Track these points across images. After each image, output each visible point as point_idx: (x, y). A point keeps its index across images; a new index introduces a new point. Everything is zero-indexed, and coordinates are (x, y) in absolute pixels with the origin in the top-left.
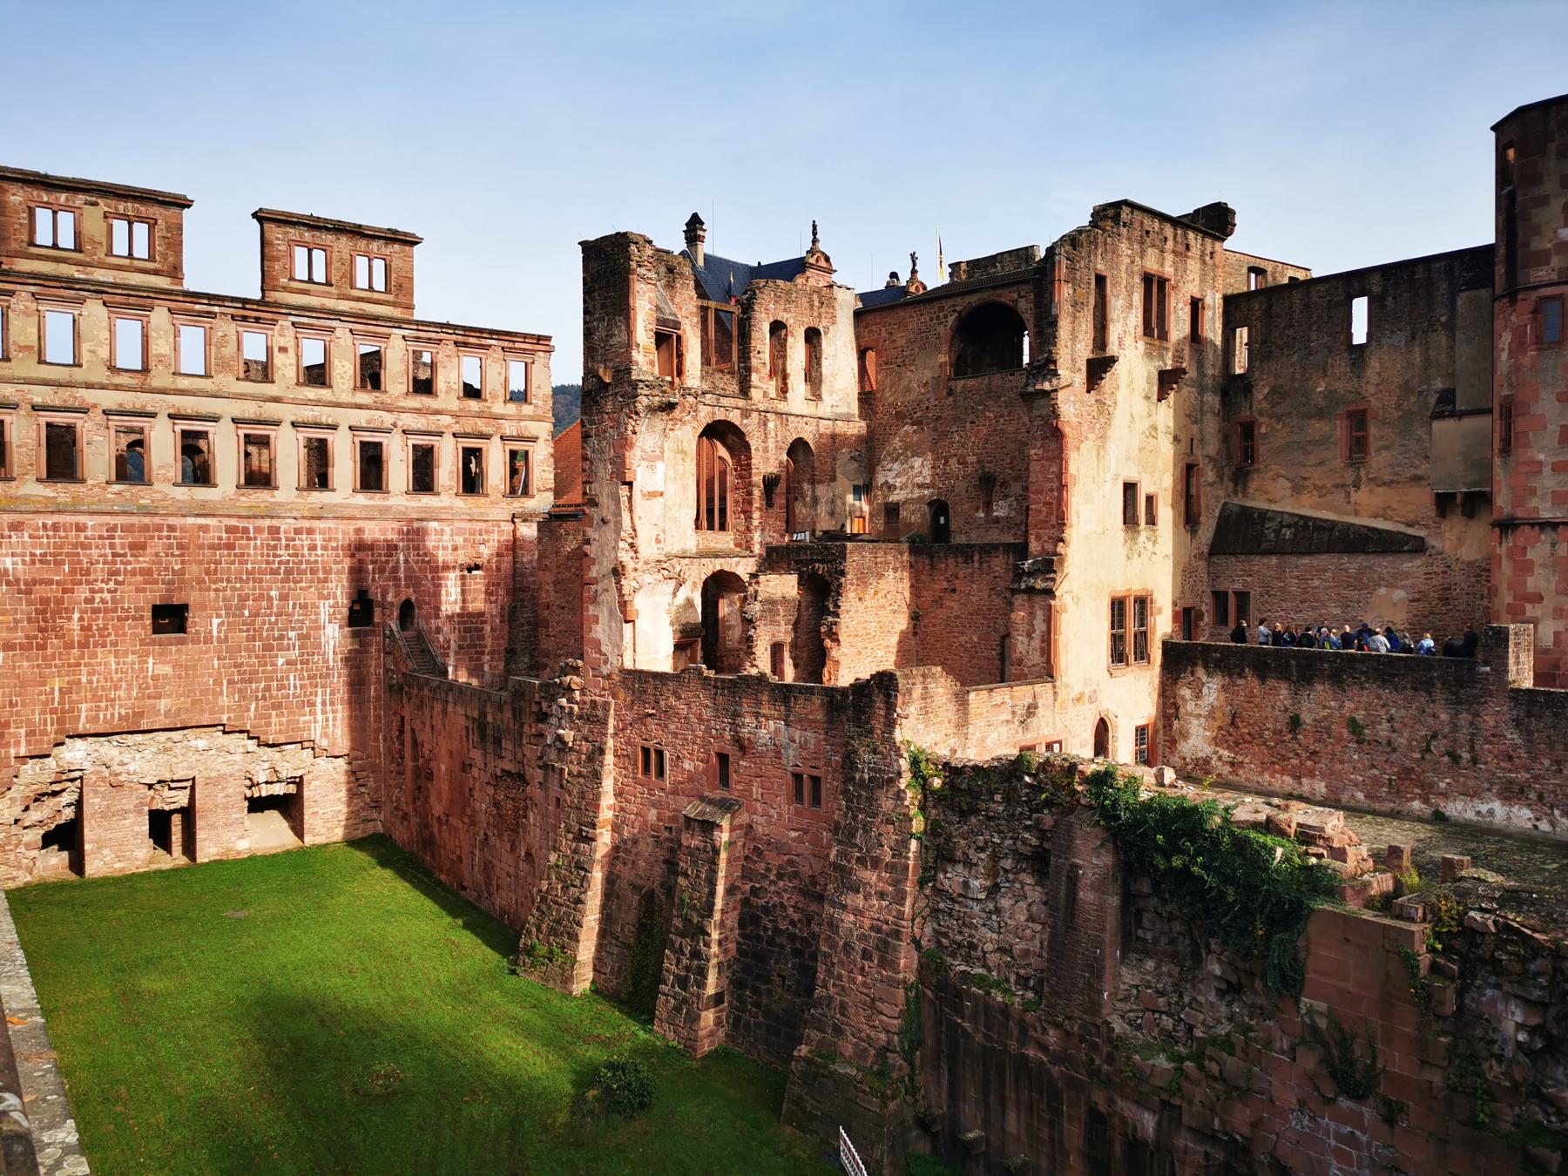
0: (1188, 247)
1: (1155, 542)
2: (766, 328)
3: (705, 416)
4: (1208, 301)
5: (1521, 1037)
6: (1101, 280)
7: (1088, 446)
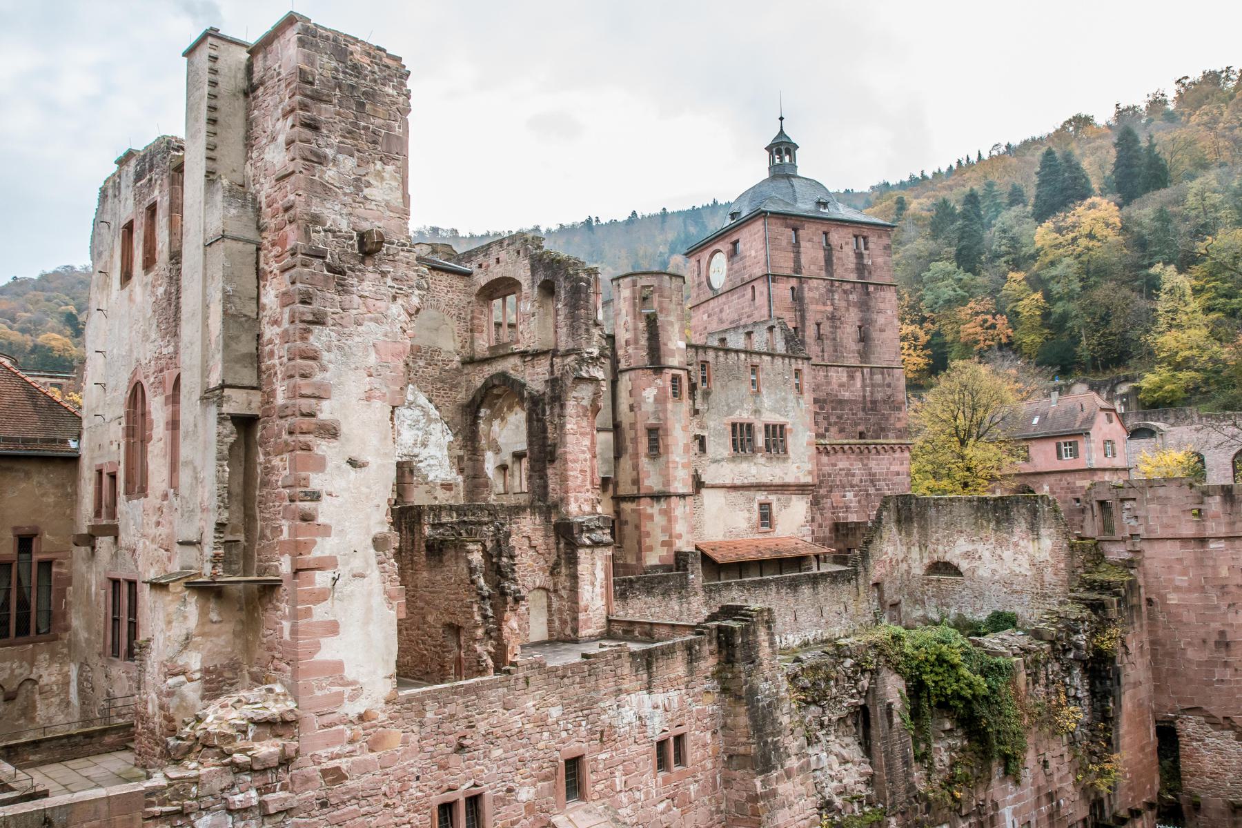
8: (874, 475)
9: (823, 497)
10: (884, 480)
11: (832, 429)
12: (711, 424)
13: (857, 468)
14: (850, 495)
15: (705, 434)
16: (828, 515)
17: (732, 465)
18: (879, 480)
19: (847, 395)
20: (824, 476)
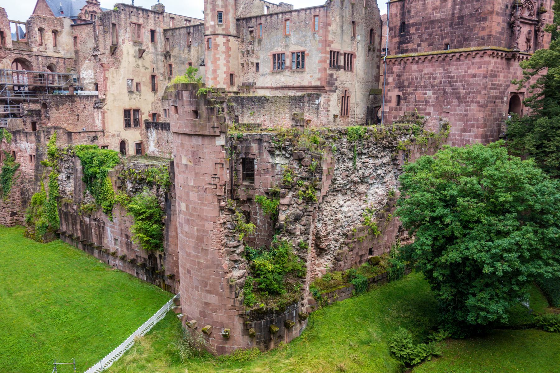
0: (148, 16)
1: (140, 96)
2: (36, 29)
3: (14, 56)
4: (158, 30)
5: (131, 189)
7: (112, 70)
8: (453, 77)
9: (409, 94)
10: (461, 81)
11: (423, 44)
12: (262, 56)
14: (430, 93)
15: (259, 62)
16: (412, 106)
17: (271, 77)
18: (456, 81)
19: (438, 15)
20: (412, 79)
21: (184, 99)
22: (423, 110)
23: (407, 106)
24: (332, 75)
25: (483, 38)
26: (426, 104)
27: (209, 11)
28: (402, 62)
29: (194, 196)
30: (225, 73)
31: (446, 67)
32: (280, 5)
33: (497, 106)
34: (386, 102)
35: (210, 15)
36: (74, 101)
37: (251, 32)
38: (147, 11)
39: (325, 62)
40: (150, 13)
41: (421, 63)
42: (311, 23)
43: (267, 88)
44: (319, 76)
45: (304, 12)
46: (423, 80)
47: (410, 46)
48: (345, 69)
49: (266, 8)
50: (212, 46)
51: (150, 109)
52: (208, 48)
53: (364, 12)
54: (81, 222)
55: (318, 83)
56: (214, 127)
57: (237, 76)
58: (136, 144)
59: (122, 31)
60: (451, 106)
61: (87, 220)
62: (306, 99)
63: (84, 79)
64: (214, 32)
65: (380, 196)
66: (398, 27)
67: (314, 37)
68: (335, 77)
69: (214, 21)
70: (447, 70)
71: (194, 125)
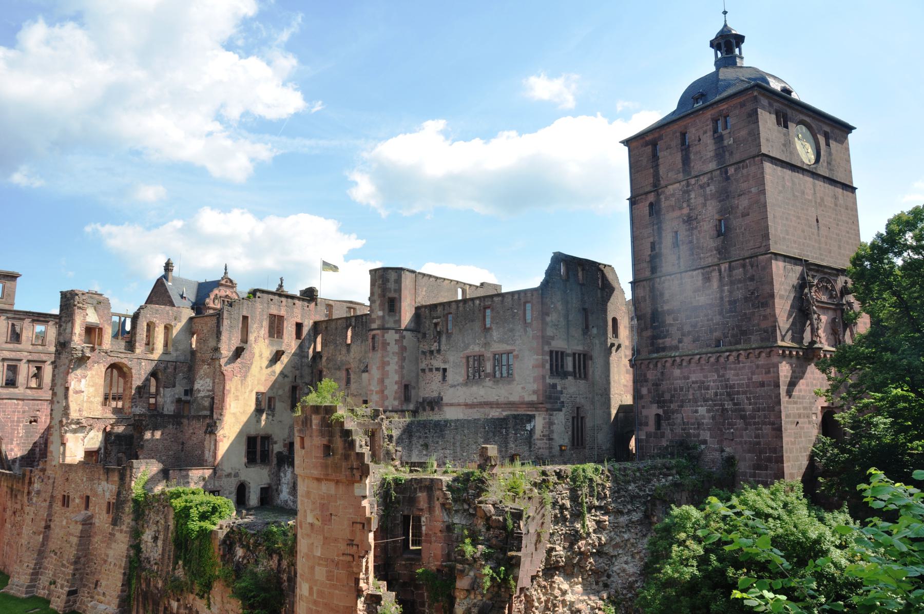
2: (145, 324)
6: (245, 318)
8: (732, 387)
9: (673, 412)
10: (745, 393)
11: (686, 339)
12: (451, 359)
13: (712, 379)
14: (702, 410)
15: (446, 366)
16: (678, 430)
17: (464, 389)
18: (738, 393)
20: (675, 390)
21: (314, 427)
22: (695, 436)
23: (672, 430)
24: (554, 386)
25: (766, 331)
26: (698, 428)
27: (376, 297)
28: (659, 365)
29: (320, 573)
30: (396, 383)
31: (721, 372)
32: (482, 284)
33: (802, 428)
34: (641, 424)
35: (378, 303)
36: (180, 424)
37: (436, 324)
38: (293, 297)
39: (543, 366)
40: (296, 301)
41: (686, 366)
42: (521, 312)
43: (459, 405)
44: (535, 387)
45: (510, 297)
46: (691, 391)
47: (668, 342)
48: (575, 376)
49: (460, 291)
50: (379, 345)
51: (286, 436)
52: (374, 348)
53: (599, 295)
54: (166, 609)
55: (534, 398)
56: (352, 469)
57: (414, 388)
58: (262, 489)
59: (255, 326)
60: (736, 430)
61: (174, 604)
62: (511, 423)
63: (199, 391)
64: (383, 325)
65: (630, 576)
66: (649, 316)
67: (526, 331)
68: (559, 388)
69: (383, 310)
70: (723, 376)
71: (325, 466)
